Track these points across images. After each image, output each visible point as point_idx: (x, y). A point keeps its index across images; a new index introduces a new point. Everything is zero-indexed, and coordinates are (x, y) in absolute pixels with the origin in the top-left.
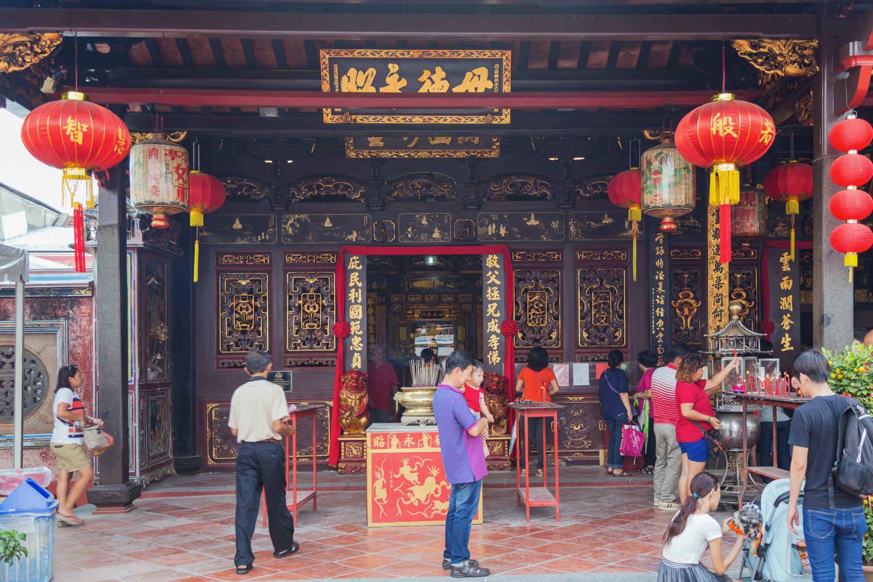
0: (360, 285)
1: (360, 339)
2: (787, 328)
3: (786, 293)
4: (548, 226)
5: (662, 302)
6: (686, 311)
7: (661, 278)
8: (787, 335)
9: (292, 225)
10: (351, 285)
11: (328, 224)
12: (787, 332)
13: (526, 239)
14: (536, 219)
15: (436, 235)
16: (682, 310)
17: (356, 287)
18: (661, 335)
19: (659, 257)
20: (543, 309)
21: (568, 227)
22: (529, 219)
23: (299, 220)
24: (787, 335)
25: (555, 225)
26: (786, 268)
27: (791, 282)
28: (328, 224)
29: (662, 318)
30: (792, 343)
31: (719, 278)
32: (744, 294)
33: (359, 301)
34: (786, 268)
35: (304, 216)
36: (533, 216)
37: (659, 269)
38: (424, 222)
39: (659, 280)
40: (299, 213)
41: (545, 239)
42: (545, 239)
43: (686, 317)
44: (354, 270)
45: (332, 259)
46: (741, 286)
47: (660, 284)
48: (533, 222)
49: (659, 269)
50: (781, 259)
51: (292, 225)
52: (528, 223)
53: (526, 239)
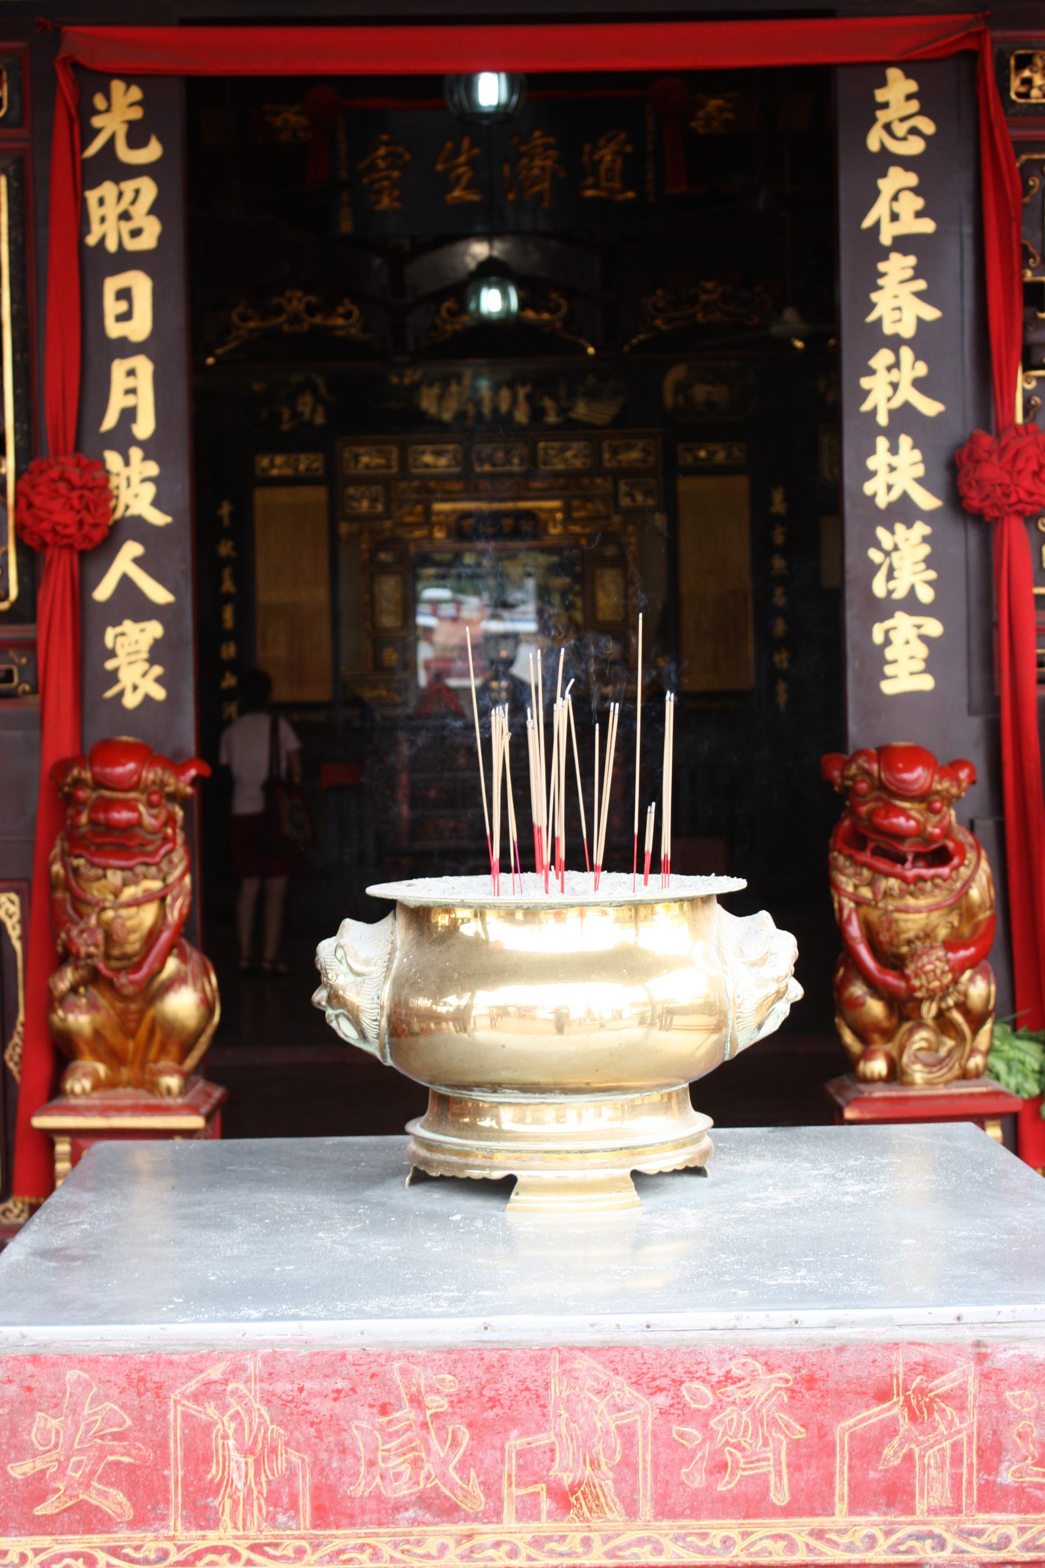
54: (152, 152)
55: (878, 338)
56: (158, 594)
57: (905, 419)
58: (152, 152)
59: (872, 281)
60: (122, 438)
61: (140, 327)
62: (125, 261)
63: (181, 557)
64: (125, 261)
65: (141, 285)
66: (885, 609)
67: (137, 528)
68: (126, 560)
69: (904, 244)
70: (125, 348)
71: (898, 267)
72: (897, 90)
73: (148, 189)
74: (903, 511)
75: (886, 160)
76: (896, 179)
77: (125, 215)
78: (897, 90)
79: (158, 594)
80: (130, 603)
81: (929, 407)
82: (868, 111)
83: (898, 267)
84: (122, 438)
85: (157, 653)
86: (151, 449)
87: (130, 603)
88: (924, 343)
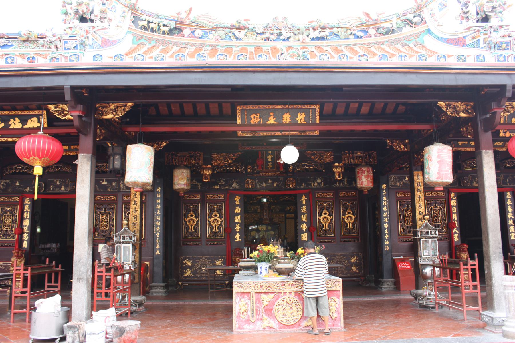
0: (29, 210)
1: (27, 234)
2: (238, 230)
3: (238, 214)
4: (111, 184)
5: (159, 219)
6: (191, 222)
7: (159, 208)
9: (3, 185)
10: (25, 210)
11: (18, 184)
12: (238, 232)
13: (101, 190)
14: (106, 181)
15: (63, 188)
16: (189, 221)
17: (27, 211)
19: (158, 198)
20: (107, 221)
21: (120, 185)
22: (103, 181)
23: (6, 183)
25: (114, 184)
27: (240, 209)
28: (18, 184)
29: (159, 226)
30: (240, 238)
31: (135, 208)
32: (218, 215)
33: (28, 217)
35: (8, 181)
37: (158, 204)
38: (58, 183)
39: (158, 209)
40: (6, 179)
43: (192, 225)
44: (27, 204)
45: (18, 199)
46: (217, 211)
47: (159, 210)
48: (105, 183)
49: (158, 204)
50: (235, 199)
51: (3, 185)
53: (101, 190)
54: (455, 198)
55: (509, 212)
56: (458, 232)
57: (511, 218)
58: (455, 198)
59: (508, 208)
60: (454, 220)
61: (455, 211)
62: (454, 206)
63: (459, 229)
64: (454, 206)
65: (455, 208)
66: (511, 233)
68: (455, 229)
69: (510, 205)
70: (454, 213)
71: (510, 207)
72: (508, 193)
73: (455, 201)
74: (512, 225)
75: (508, 198)
76: (509, 200)
77: (453, 203)
78: (508, 193)
79: (458, 232)
80: (456, 233)
81: (513, 217)
82: (506, 195)
83: (510, 207)
85: (458, 237)
87: (456, 233)
88: (512, 212)
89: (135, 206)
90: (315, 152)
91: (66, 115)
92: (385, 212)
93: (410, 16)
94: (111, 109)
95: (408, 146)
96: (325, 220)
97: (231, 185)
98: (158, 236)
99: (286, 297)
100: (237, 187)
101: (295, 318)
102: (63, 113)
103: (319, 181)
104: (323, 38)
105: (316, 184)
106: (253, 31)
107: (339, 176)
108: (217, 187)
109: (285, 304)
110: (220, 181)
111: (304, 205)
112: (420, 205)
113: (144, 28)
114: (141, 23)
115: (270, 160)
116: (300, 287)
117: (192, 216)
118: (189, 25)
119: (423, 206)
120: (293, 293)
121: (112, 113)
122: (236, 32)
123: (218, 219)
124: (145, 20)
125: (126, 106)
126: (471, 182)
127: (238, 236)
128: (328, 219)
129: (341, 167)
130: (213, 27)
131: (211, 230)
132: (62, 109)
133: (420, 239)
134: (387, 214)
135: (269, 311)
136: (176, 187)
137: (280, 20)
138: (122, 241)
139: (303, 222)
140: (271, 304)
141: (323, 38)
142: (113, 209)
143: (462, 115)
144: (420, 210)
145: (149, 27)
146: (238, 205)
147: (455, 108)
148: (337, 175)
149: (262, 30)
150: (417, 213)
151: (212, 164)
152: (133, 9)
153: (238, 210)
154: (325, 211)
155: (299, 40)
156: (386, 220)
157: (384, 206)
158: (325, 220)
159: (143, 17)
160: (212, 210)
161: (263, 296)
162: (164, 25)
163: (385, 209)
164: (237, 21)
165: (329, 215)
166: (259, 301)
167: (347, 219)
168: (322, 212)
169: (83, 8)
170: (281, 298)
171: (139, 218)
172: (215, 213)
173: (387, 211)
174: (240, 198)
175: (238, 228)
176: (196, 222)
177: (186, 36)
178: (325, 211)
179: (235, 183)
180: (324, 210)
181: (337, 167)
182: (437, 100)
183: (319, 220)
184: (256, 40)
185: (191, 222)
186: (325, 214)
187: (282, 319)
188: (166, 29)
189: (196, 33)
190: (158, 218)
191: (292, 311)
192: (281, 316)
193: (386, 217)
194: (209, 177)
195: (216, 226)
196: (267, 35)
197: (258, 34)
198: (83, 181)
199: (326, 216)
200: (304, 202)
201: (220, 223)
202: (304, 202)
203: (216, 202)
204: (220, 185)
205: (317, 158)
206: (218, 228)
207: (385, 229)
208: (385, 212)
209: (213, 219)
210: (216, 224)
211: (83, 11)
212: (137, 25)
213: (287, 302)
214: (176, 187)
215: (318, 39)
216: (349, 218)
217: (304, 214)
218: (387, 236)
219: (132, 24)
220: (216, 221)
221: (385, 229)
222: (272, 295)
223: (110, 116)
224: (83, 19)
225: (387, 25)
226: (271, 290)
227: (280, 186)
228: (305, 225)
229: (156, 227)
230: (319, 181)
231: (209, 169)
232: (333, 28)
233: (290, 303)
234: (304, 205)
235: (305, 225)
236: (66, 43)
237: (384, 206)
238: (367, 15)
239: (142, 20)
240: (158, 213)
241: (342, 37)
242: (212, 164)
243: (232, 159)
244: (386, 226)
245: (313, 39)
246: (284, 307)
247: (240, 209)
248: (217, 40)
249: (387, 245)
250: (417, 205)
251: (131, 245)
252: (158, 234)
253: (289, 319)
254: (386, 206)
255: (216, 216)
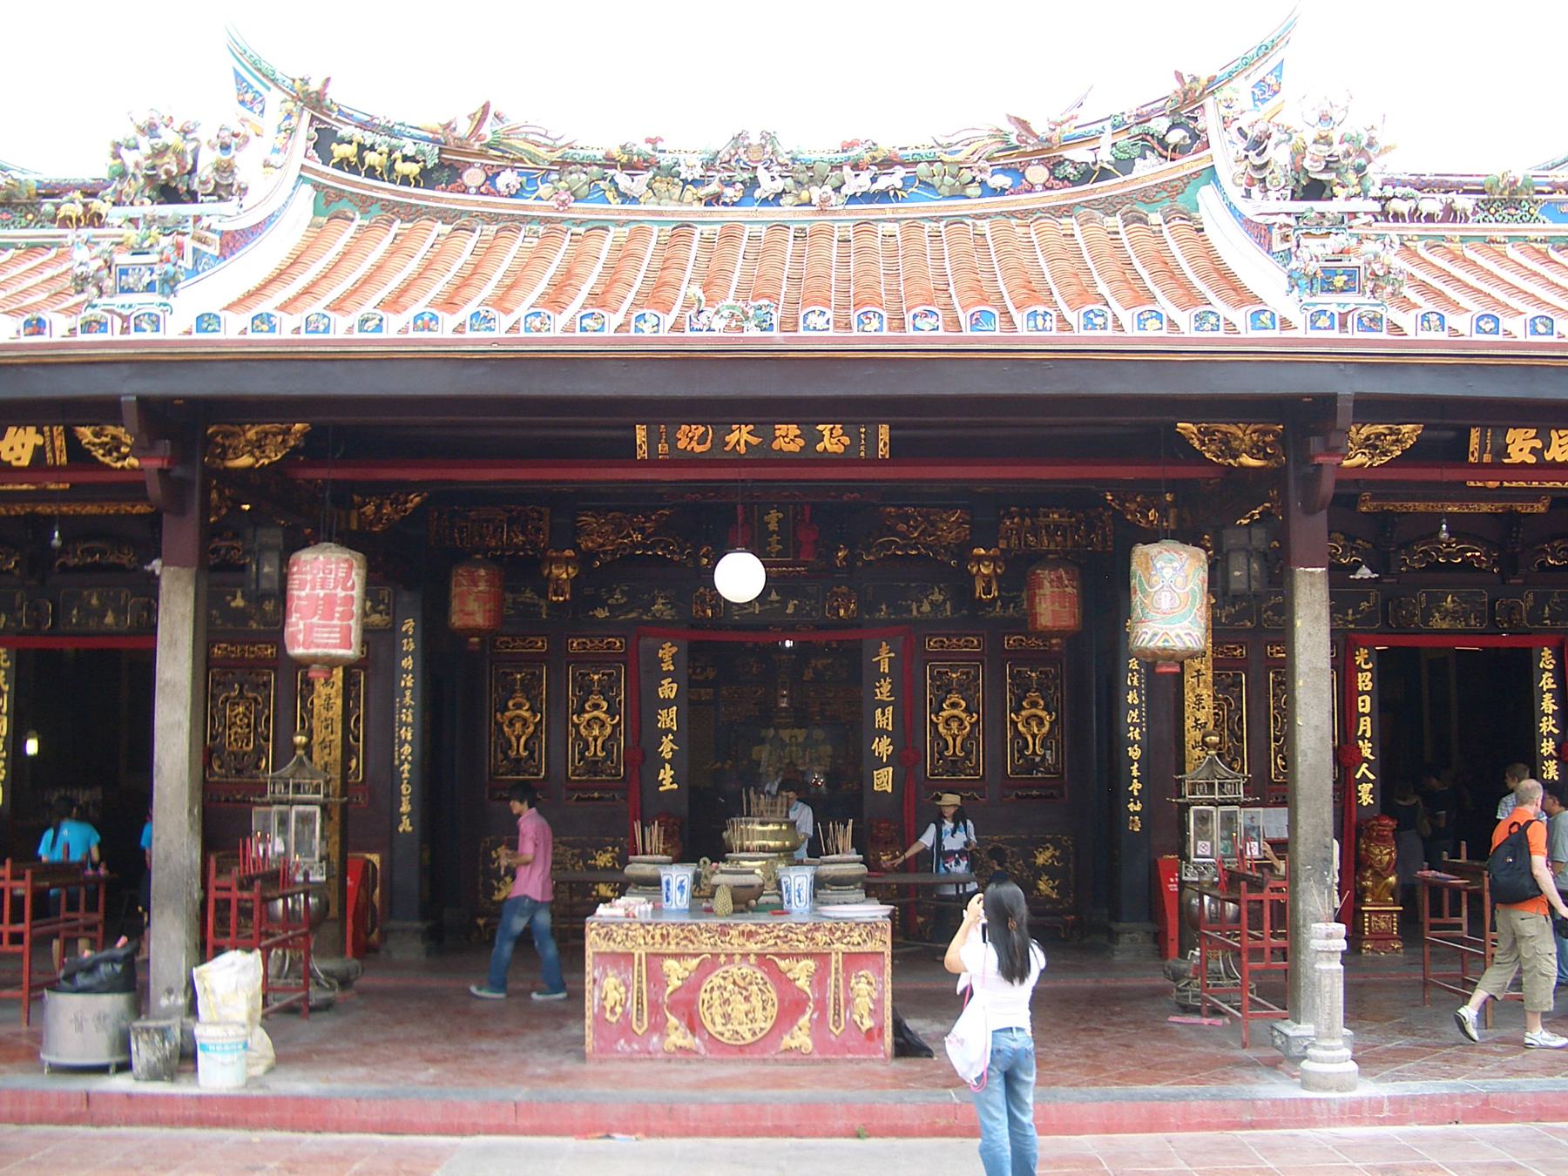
3: (667, 704)
4: (260, 608)
5: (410, 719)
6: (518, 725)
8: (667, 766)
12: (668, 761)
15: (109, 619)
16: (511, 724)
18: (406, 767)
19: (406, 654)
22: (235, 598)
24: (667, 766)
26: (668, 666)
27: (675, 686)
30: (674, 779)
31: (329, 697)
34: (668, 666)
36: (239, 594)
37: (407, 672)
38: (94, 601)
39: (406, 688)
41: (254, 626)
42: (254, 626)
46: (600, 693)
47: (408, 693)
48: (239, 602)
49: (407, 672)
52: (233, 604)
53: (230, 626)
54: (1370, 666)
55: (1544, 714)
56: (1372, 777)
58: (1370, 666)
61: (1367, 710)
67: (1366, 760)
69: (1549, 691)
70: (1364, 714)
71: (1548, 696)
72: (1547, 652)
75: (1545, 670)
78: (1547, 652)
79: (1372, 777)
80: (1365, 779)
83: (1548, 696)
84: (1363, 738)
86: (1370, 740)
87: (1365, 779)
89: (328, 690)
90: (911, 510)
91: (125, 457)
92: (1133, 707)
93: (1159, 125)
94: (248, 442)
95: (1172, 513)
96: (954, 725)
97: (647, 610)
98: (406, 775)
99: (734, 969)
100: (667, 615)
101: (756, 1026)
102: (118, 449)
103: (937, 597)
104: (883, 196)
105: (926, 608)
106: (671, 173)
107: (987, 591)
108: (601, 614)
109: (730, 987)
110: (611, 593)
111: (884, 676)
112: (1199, 698)
113: (343, 164)
114: (340, 151)
115: (773, 526)
116: (772, 942)
117: (519, 706)
118: (480, 155)
119: (1208, 702)
120: (752, 959)
121: (252, 454)
122: (622, 179)
123: (603, 716)
124: (350, 143)
125: (288, 432)
126: (1426, 616)
127: (666, 774)
128: (961, 721)
129: (993, 559)
130: (552, 163)
131: (582, 753)
132: (114, 437)
133: (1188, 805)
134: (1139, 716)
135: (688, 1009)
136: (457, 620)
137: (755, 140)
138: (291, 796)
139: (882, 732)
140: (692, 986)
141: (883, 196)
142: (266, 685)
143: (1247, 460)
144: (1198, 715)
145: (362, 160)
146: (668, 674)
147: (1226, 440)
148: (979, 586)
149: (698, 173)
150: (1189, 723)
151: (576, 547)
152: (315, 102)
153: (668, 690)
154: (955, 698)
155: (810, 203)
156: (1135, 734)
157: (1132, 688)
158: (954, 725)
159: (345, 131)
160: (586, 689)
161: (670, 964)
162: (405, 159)
163: (1132, 697)
164: (623, 147)
165: (967, 710)
166: (656, 978)
167: (1027, 723)
168: (943, 701)
169: (170, 164)
170: (720, 972)
171: (338, 727)
172: (594, 698)
173: (1138, 706)
174: (674, 650)
175: (667, 748)
176: (532, 728)
177: (473, 190)
178: (955, 698)
179: (660, 601)
180: (949, 692)
181: (980, 560)
182: (1173, 418)
183: (934, 725)
184: (680, 200)
185: (518, 725)
186: (954, 705)
187: (720, 1028)
188: (412, 169)
189: (501, 182)
190: (407, 716)
191: (746, 1007)
192: (719, 1020)
193: (1135, 725)
194: (567, 589)
195: (596, 739)
196: (713, 188)
197: (685, 182)
198: (173, 643)
199: (956, 712)
200: (885, 668)
201: (609, 730)
202: (885, 668)
203: (598, 661)
204: (612, 608)
205: (916, 528)
206: (603, 749)
207: (1132, 762)
208: (1133, 707)
209: (587, 716)
210: (596, 732)
211: (168, 172)
212: (326, 157)
213: (734, 983)
214: (457, 620)
215: (867, 197)
216: (1034, 725)
217: (883, 705)
218: (1136, 786)
219: (312, 152)
220: (596, 725)
221: (1132, 762)
222: (696, 962)
223: (245, 461)
224: (168, 193)
225: (1080, 155)
226: (691, 949)
227: (809, 614)
228: (886, 741)
229: (401, 746)
230: (937, 597)
231: (568, 561)
232: (916, 163)
233: (742, 984)
234: (884, 676)
235: (886, 741)
236: (124, 272)
237: (1132, 688)
238: (1023, 124)
239: (341, 141)
240: (408, 700)
241: (945, 190)
242: (576, 547)
243: (642, 530)
244: (1135, 753)
245: (853, 199)
246: (726, 995)
247: (675, 686)
248: (564, 203)
249: (1135, 813)
250: (1190, 699)
251: (318, 809)
252: (406, 767)
253: (740, 1029)
254: (1138, 689)
255: (596, 706)
